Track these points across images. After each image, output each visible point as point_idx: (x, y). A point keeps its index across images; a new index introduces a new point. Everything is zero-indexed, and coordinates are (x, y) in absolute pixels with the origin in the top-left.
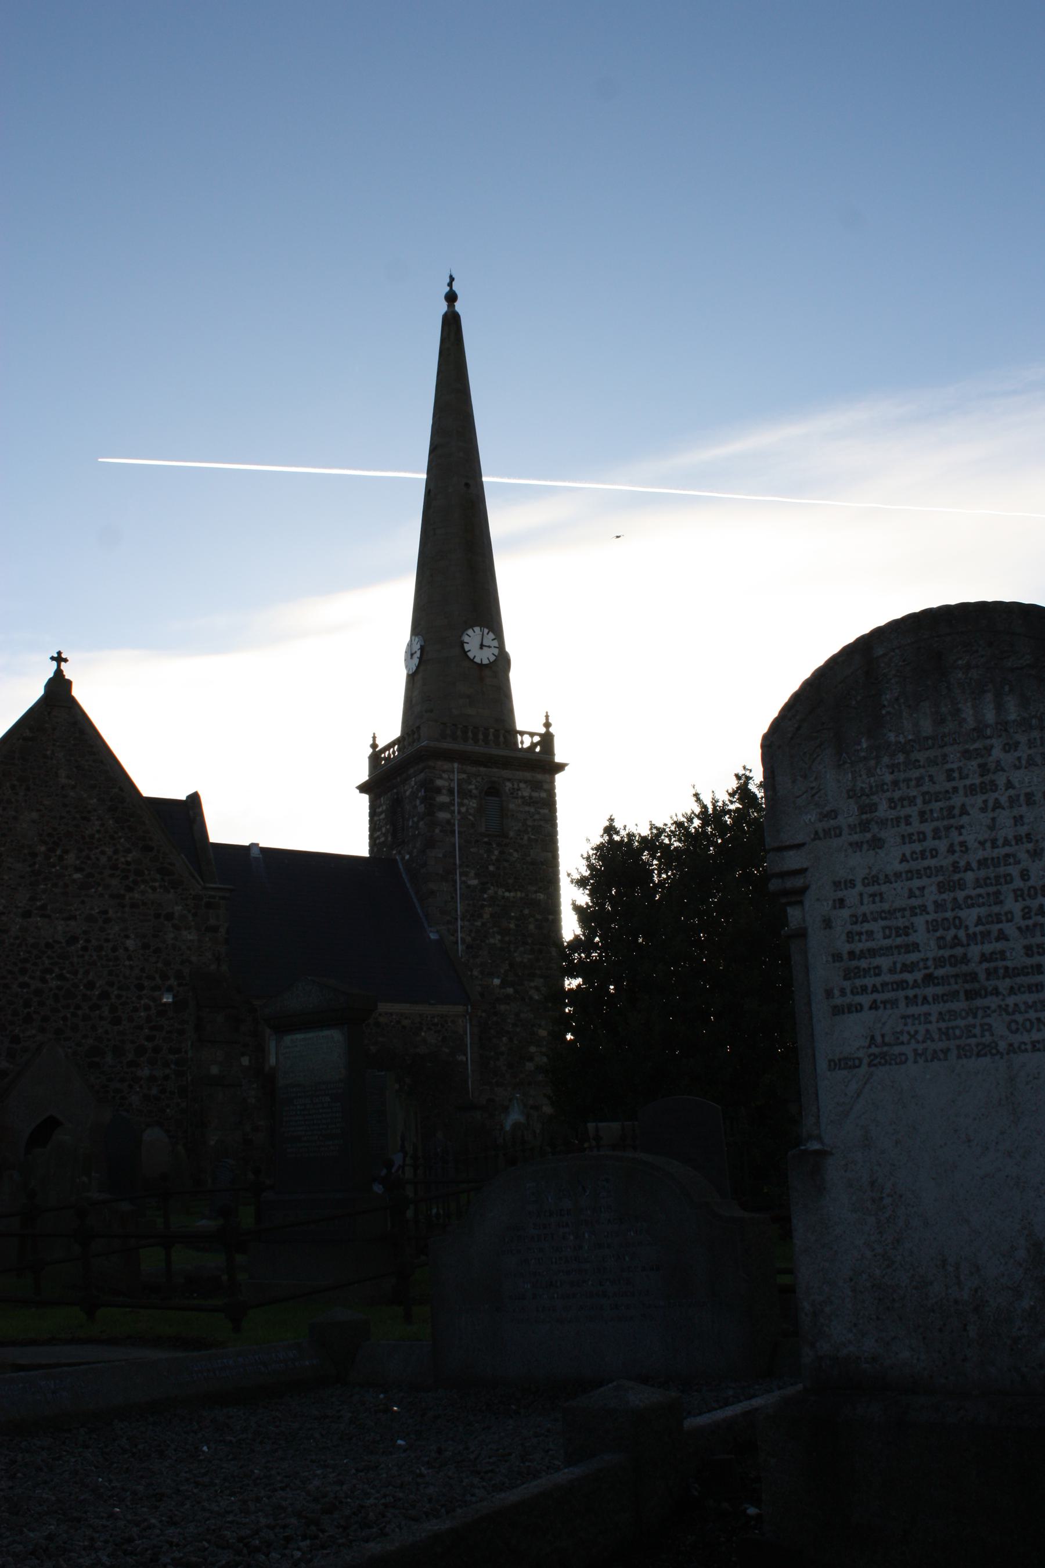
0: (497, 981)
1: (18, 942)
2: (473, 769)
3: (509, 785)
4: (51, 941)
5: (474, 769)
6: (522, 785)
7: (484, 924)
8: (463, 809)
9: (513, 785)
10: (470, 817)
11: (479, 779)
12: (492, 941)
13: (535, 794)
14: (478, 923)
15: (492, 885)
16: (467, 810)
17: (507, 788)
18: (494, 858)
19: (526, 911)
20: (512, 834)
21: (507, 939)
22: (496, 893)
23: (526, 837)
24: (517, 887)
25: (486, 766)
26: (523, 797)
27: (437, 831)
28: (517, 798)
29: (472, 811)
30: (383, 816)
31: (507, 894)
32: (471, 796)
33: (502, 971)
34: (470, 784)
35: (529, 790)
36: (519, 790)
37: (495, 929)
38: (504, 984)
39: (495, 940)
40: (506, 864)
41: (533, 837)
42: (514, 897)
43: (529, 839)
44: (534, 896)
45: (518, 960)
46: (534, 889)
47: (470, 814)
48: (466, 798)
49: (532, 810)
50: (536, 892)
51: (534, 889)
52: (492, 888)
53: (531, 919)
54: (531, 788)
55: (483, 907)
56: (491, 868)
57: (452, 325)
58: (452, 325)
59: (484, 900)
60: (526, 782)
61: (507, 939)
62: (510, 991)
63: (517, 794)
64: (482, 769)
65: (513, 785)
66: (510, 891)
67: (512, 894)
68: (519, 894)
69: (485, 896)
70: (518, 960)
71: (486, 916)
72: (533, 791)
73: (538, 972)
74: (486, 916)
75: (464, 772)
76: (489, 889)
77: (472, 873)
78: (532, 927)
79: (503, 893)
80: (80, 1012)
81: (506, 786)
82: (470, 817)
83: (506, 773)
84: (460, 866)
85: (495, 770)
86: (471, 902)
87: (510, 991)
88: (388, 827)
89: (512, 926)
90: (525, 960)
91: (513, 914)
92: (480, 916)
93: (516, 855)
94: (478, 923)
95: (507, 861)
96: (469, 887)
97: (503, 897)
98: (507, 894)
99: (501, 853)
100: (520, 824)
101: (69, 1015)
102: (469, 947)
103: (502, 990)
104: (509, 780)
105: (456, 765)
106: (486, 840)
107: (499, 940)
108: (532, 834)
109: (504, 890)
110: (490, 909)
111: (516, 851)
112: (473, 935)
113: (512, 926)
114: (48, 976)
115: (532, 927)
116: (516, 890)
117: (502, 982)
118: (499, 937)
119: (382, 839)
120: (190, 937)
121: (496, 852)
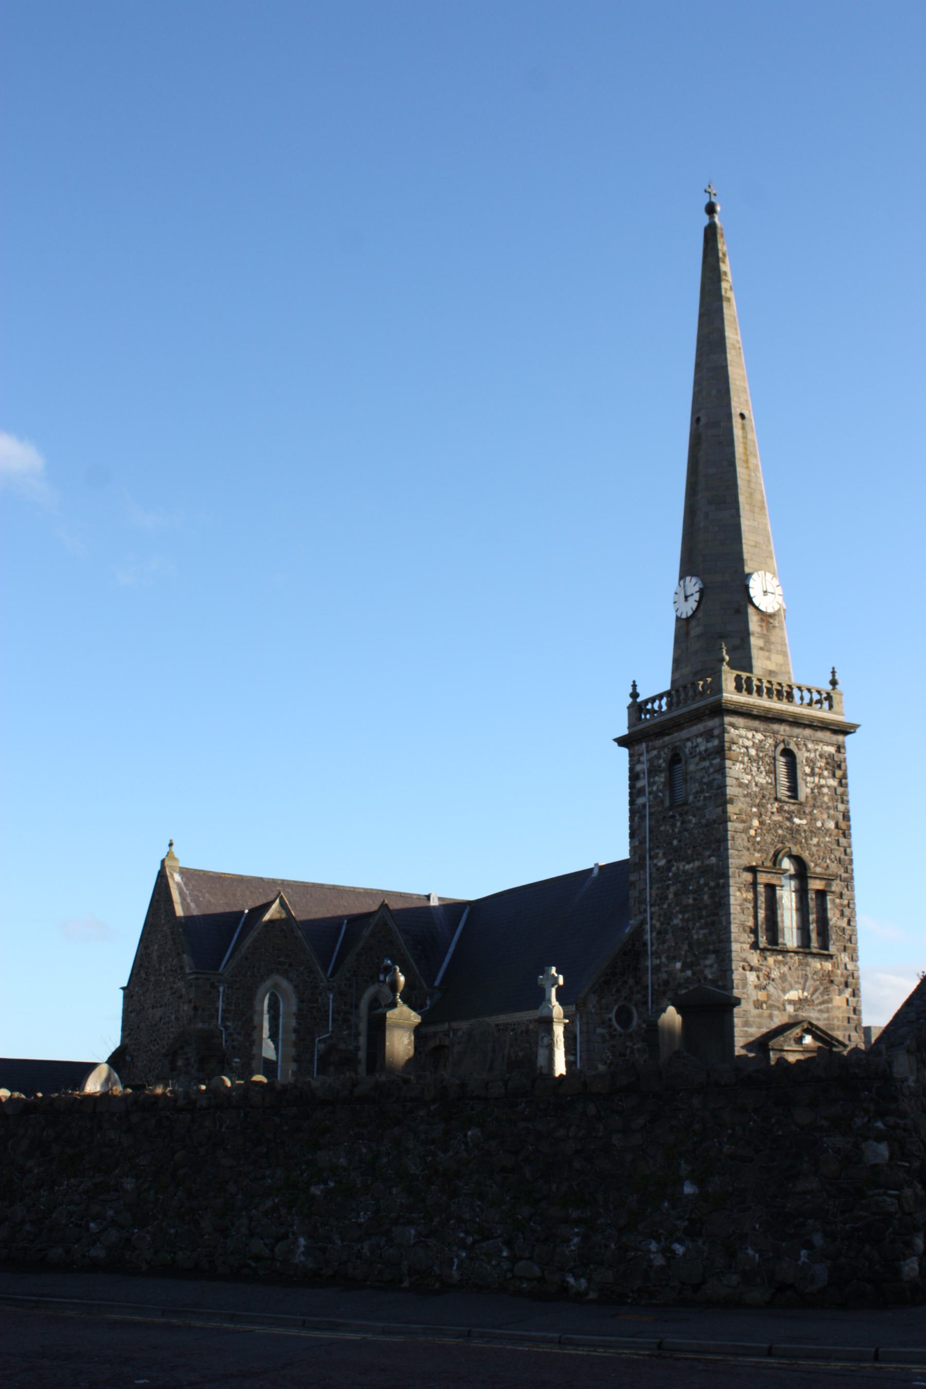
0: (678, 965)
2: (658, 743)
3: (689, 744)
5: (661, 741)
6: (699, 740)
7: (669, 905)
8: (655, 788)
9: (692, 743)
10: (660, 794)
11: (666, 750)
13: (710, 745)
14: (665, 906)
15: (676, 860)
16: (658, 787)
17: (687, 751)
18: (677, 830)
21: (686, 916)
22: (678, 868)
23: (702, 798)
24: (695, 857)
25: (668, 734)
26: (700, 753)
28: (695, 756)
29: (661, 787)
31: (687, 867)
32: (660, 772)
33: (683, 953)
34: (660, 758)
35: (705, 743)
36: (697, 746)
40: (686, 834)
41: (707, 795)
42: (692, 869)
43: (705, 798)
47: (660, 791)
48: (657, 775)
49: (706, 764)
50: (710, 856)
52: (675, 864)
53: (706, 889)
54: (707, 739)
55: (668, 887)
56: (675, 842)
57: (711, 234)
58: (711, 234)
59: (669, 879)
60: (701, 735)
61: (686, 916)
63: (695, 752)
64: (667, 738)
65: (692, 743)
66: (688, 863)
67: (691, 865)
68: (697, 863)
69: (671, 874)
70: (695, 937)
71: (671, 896)
72: (708, 741)
73: (711, 947)
74: (671, 896)
75: (654, 749)
76: (673, 866)
77: (661, 855)
78: (706, 897)
79: (684, 866)
81: (686, 747)
82: (660, 794)
83: (684, 734)
84: (650, 849)
85: (676, 734)
86: (660, 885)
87: (689, 973)
89: (691, 901)
90: (701, 936)
91: (691, 888)
92: (666, 898)
94: (665, 906)
95: (686, 830)
96: (658, 869)
97: (684, 872)
98: (687, 867)
99: (683, 823)
100: (697, 785)
102: (659, 933)
103: (683, 974)
104: (688, 739)
105: (644, 745)
106: (671, 813)
107: (680, 920)
108: (707, 792)
109: (684, 863)
110: (674, 887)
111: (694, 816)
115: (706, 897)
116: (693, 861)
117: (683, 966)
118: (680, 916)
121: (679, 824)
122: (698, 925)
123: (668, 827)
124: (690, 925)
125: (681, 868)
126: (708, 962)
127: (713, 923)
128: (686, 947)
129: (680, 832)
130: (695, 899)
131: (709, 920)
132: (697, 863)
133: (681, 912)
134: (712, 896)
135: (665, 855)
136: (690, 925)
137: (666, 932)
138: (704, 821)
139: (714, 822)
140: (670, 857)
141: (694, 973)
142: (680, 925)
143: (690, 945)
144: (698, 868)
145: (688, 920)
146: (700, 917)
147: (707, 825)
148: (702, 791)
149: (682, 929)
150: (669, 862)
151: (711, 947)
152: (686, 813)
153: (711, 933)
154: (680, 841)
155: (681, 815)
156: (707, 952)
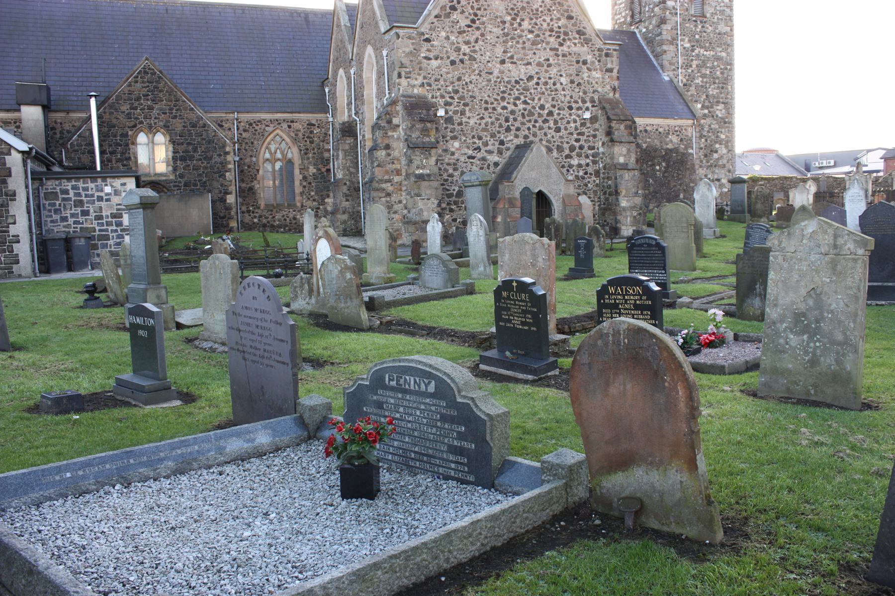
1: (499, 80)
4: (518, 79)
7: (692, 71)
12: (697, 81)
14: (690, 71)
18: (698, 30)
19: (716, 64)
20: (708, 15)
21: (705, 80)
23: (716, 17)
27: (667, 13)
30: (623, 5)
37: (699, 74)
38: (703, 107)
39: (699, 81)
40: (705, 34)
44: (720, 54)
45: (711, 93)
46: (720, 49)
51: (720, 49)
53: (718, 68)
55: (692, 60)
56: (697, 37)
61: (705, 80)
62: (706, 111)
67: (708, 53)
70: (711, 93)
71: (694, 66)
73: (721, 100)
74: (694, 66)
77: (687, 40)
78: (718, 73)
80: (537, 125)
87: (706, 111)
88: (627, 12)
89: (708, 72)
92: (691, 66)
93: (710, 28)
94: (690, 71)
95: (705, 32)
96: (684, 48)
98: (705, 53)
99: (703, 27)
101: (531, 127)
106: (694, 19)
112: (687, 77)
113: (708, 72)
114: (518, 102)
117: (702, 106)
118: (700, 79)
119: (623, 20)
120: (597, 76)
121: (700, 27)
122: (712, 86)
123: (692, 26)
124: (708, 85)
125: (702, 52)
126: (719, 108)
127: (723, 88)
128: (704, 97)
129: (700, 32)
130: (711, 72)
131: (721, 85)
132: (712, 53)
133: (701, 76)
134: (722, 73)
135: (689, 41)
136: (708, 85)
137: (690, 86)
138: (717, 31)
139: (725, 34)
140: (693, 44)
141: (710, 112)
142: (701, 84)
143: (707, 96)
144: (713, 56)
145: (706, 82)
146: (714, 83)
147: (719, 34)
148: (716, 14)
149: (702, 86)
150: (693, 46)
151: (721, 100)
152: (705, 22)
153: (721, 93)
154: (701, 37)
155: (701, 22)
156: (718, 102)
